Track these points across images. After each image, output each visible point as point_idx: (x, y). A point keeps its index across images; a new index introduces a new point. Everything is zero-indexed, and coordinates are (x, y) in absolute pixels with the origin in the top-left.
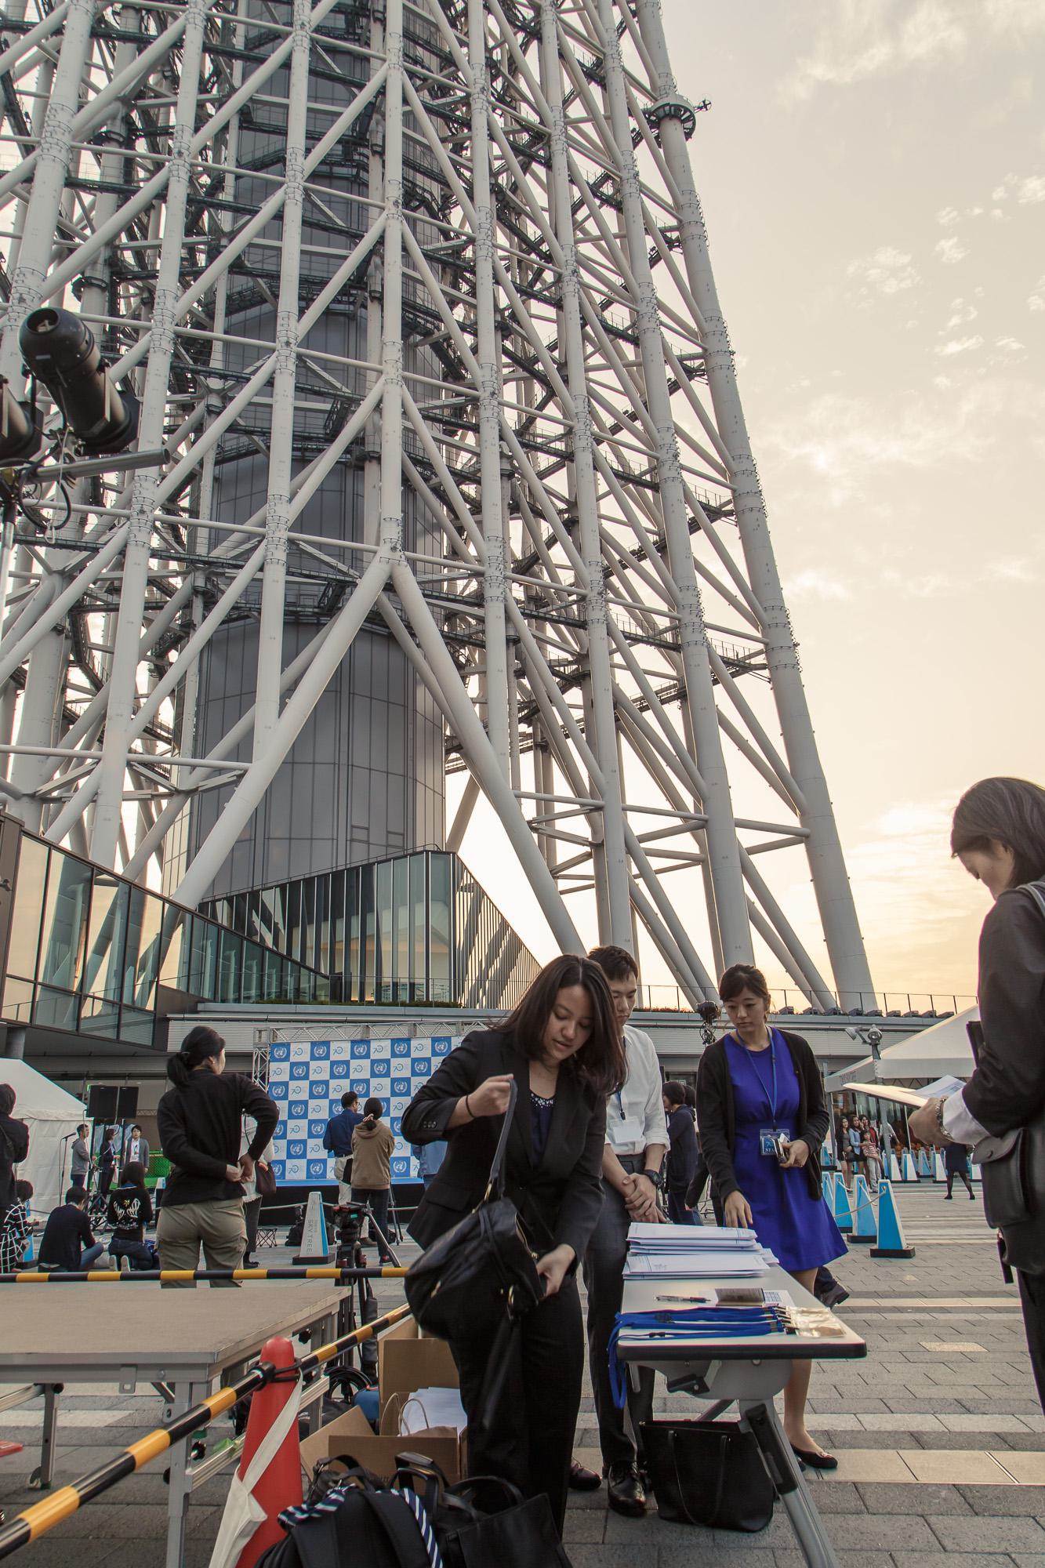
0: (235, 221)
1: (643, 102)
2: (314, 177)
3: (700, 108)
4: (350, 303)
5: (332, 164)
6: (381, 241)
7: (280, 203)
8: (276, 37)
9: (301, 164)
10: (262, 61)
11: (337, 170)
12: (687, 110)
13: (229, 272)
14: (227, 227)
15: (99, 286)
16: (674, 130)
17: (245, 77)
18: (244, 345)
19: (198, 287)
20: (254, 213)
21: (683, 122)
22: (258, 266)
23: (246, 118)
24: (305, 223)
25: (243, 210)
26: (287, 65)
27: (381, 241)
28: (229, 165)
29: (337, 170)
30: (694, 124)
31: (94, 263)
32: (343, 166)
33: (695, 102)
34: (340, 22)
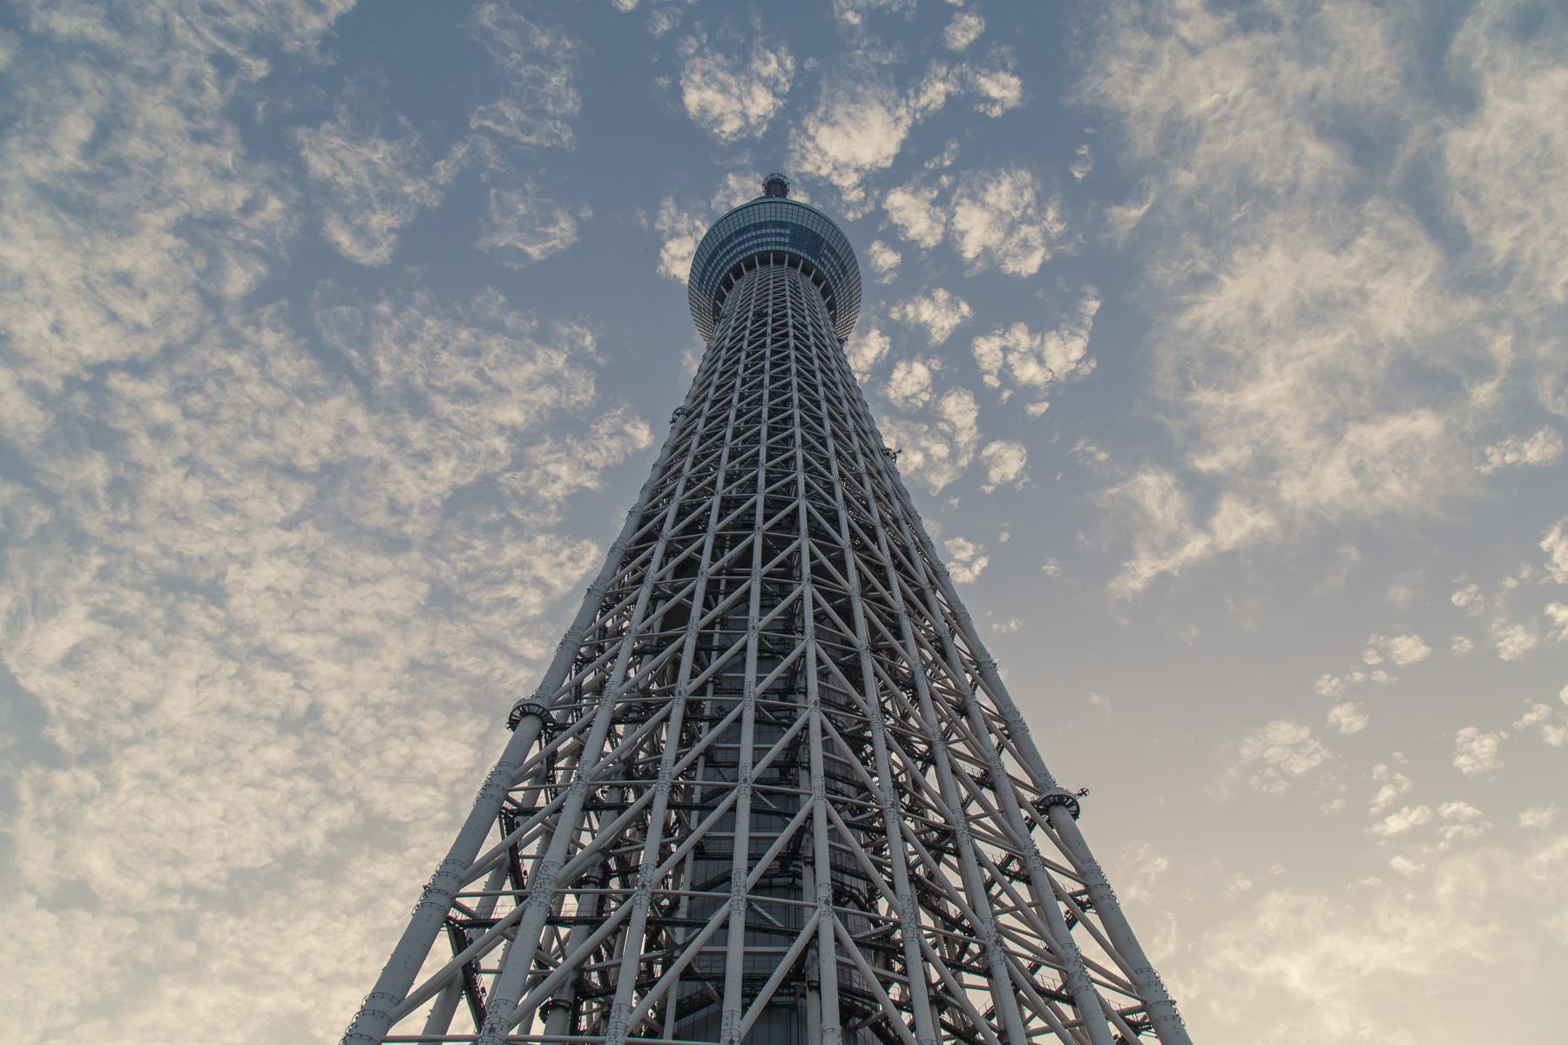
0: (687, 933)
1: (1029, 796)
2: (756, 888)
3: (1080, 795)
4: (791, 995)
6: (816, 935)
8: (727, 790)
9: (743, 879)
10: (713, 808)
11: (776, 881)
12: (1068, 798)
13: (680, 980)
14: (679, 940)
15: (563, 1007)
16: (1061, 814)
17: (700, 821)
19: (653, 994)
20: (703, 925)
21: (1068, 806)
22: (708, 971)
23: (700, 851)
24: (747, 928)
25: (694, 924)
26: (733, 809)
27: (816, 935)
29: (776, 881)
30: (1078, 807)
31: (562, 986)
33: (1074, 791)
34: (776, 773)
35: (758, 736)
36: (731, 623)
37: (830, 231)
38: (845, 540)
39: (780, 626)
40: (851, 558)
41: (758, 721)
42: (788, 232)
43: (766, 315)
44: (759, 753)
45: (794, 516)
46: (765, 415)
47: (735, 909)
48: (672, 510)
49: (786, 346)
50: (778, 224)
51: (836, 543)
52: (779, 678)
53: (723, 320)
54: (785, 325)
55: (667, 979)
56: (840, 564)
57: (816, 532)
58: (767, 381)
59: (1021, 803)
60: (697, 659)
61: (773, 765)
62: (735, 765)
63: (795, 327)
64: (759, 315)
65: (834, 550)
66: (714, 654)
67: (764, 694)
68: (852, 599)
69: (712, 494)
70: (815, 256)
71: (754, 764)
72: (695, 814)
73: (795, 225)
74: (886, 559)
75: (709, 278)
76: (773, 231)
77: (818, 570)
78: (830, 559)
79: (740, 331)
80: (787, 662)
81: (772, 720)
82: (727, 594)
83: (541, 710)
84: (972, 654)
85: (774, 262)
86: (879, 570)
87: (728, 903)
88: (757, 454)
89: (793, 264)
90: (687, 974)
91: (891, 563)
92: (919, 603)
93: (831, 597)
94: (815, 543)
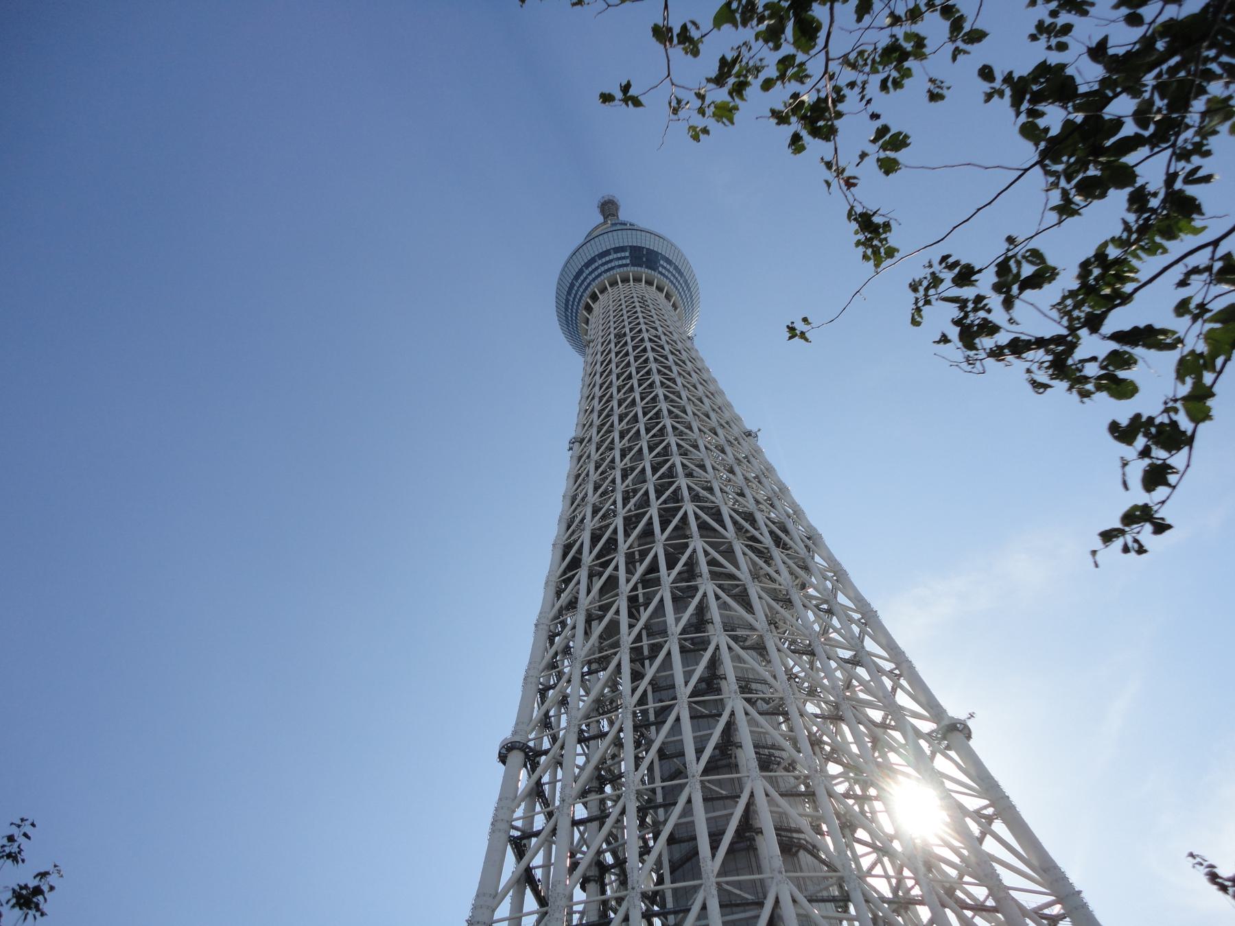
0: (666, 812)
2: (706, 772)
5: (717, 761)
7: (688, 794)
8: (671, 707)
9: (695, 767)
10: (664, 722)
11: (720, 763)
13: (668, 845)
14: (661, 818)
17: (658, 732)
18: (685, 888)
19: (651, 859)
20: (675, 804)
22: (686, 835)
23: (662, 753)
25: (669, 805)
26: (678, 719)
28: (658, 784)
29: (720, 763)
32: (722, 760)
34: (704, 685)
35: (685, 663)
36: (650, 580)
39: (685, 575)
41: (683, 650)
42: (627, 254)
44: (688, 676)
46: (636, 385)
47: (693, 790)
49: (645, 350)
50: (617, 250)
52: (692, 615)
55: (659, 846)
58: (634, 372)
60: (631, 615)
61: (701, 680)
62: (673, 687)
63: (650, 340)
66: (642, 609)
67: (684, 631)
71: (686, 683)
72: (653, 728)
76: (615, 256)
79: (607, 365)
80: (695, 602)
81: (693, 646)
82: (641, 561)
85: (622, 282)
87: (688, 786)
89: (637, 280)
90: (671, 840)
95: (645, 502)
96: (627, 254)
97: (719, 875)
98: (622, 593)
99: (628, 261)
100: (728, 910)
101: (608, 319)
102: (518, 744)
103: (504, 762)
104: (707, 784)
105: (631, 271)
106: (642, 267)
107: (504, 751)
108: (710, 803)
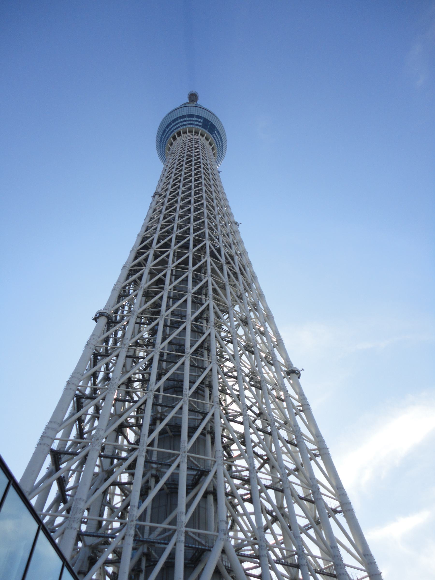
1: (285, 369)
16: (294, 376)
37: (217, 121)
38: (223, 260)
40: (225, 268)
42: (202, 121)
43: (192, 156)
45: (204, 247)
48: (156, 237)
51: (219, 261)
53: (173, 155)
54: (200, 167)
56: (221, 269)
57: (212, 255)
59: (282, 370)
64: (189, 156)
65: (219, 263)
68: (226, 285)
69: (172, 233)
70: (212, 134)
73: (205, 118)
74: (237, 270)
75: (167, 134)
77: (213, 270)
78: (217, 267)
83: (108, 315)
84: (268, 316)
86: (235, 274)
88: (189, 229)
89: (202, 135)
91: (239, 272)
92: (248, 287)
93: (217, 283)
94: (212, 260)
95: (187, 232)
96: (202, 121)
97: (190, 397)
98: (169, 267)
99: (201, 124)
100: (192, 413)
101: (184, 149)
102: (106, 314)
103: (96, 321)
104: (192, 359)
105: (201, 130)
106: (206, 130)
107: (98, 315)
108: (193, 368)
